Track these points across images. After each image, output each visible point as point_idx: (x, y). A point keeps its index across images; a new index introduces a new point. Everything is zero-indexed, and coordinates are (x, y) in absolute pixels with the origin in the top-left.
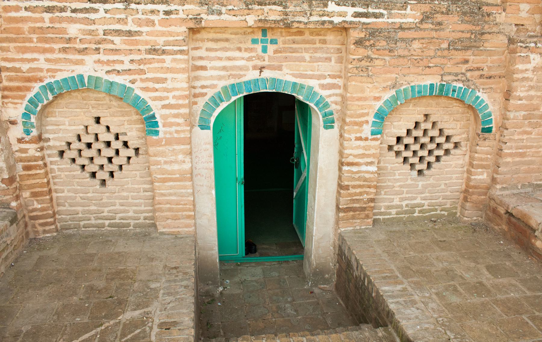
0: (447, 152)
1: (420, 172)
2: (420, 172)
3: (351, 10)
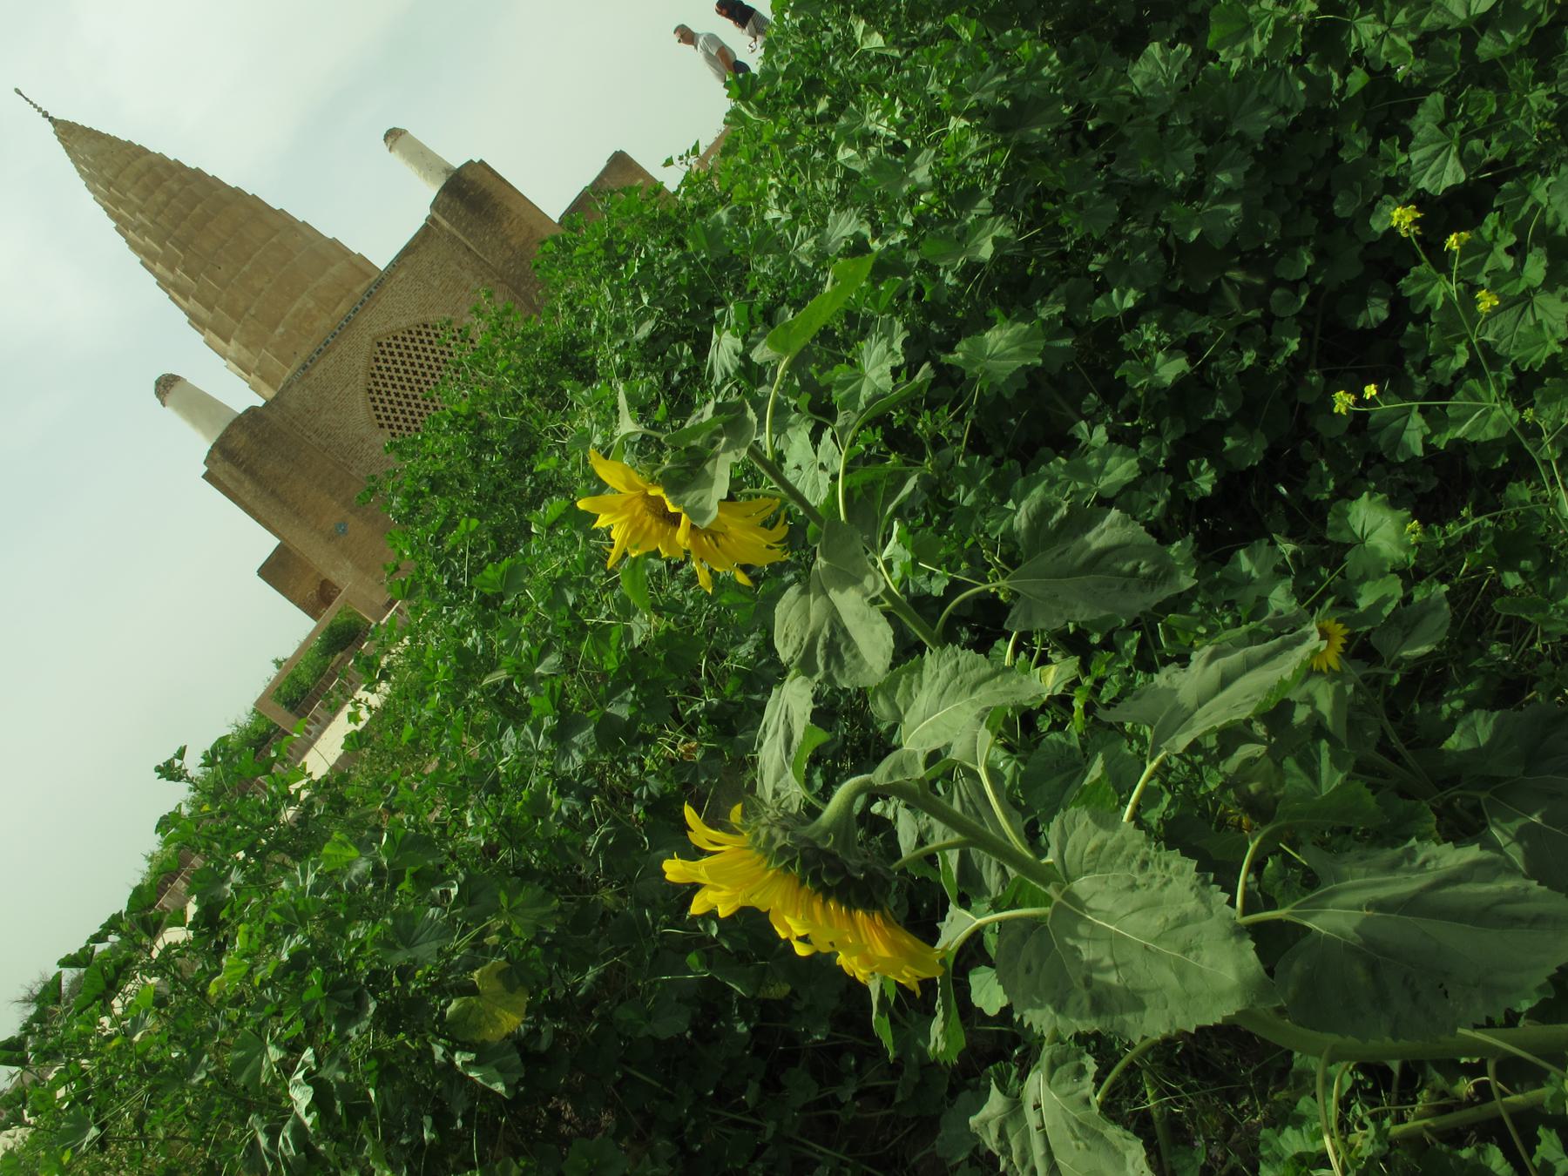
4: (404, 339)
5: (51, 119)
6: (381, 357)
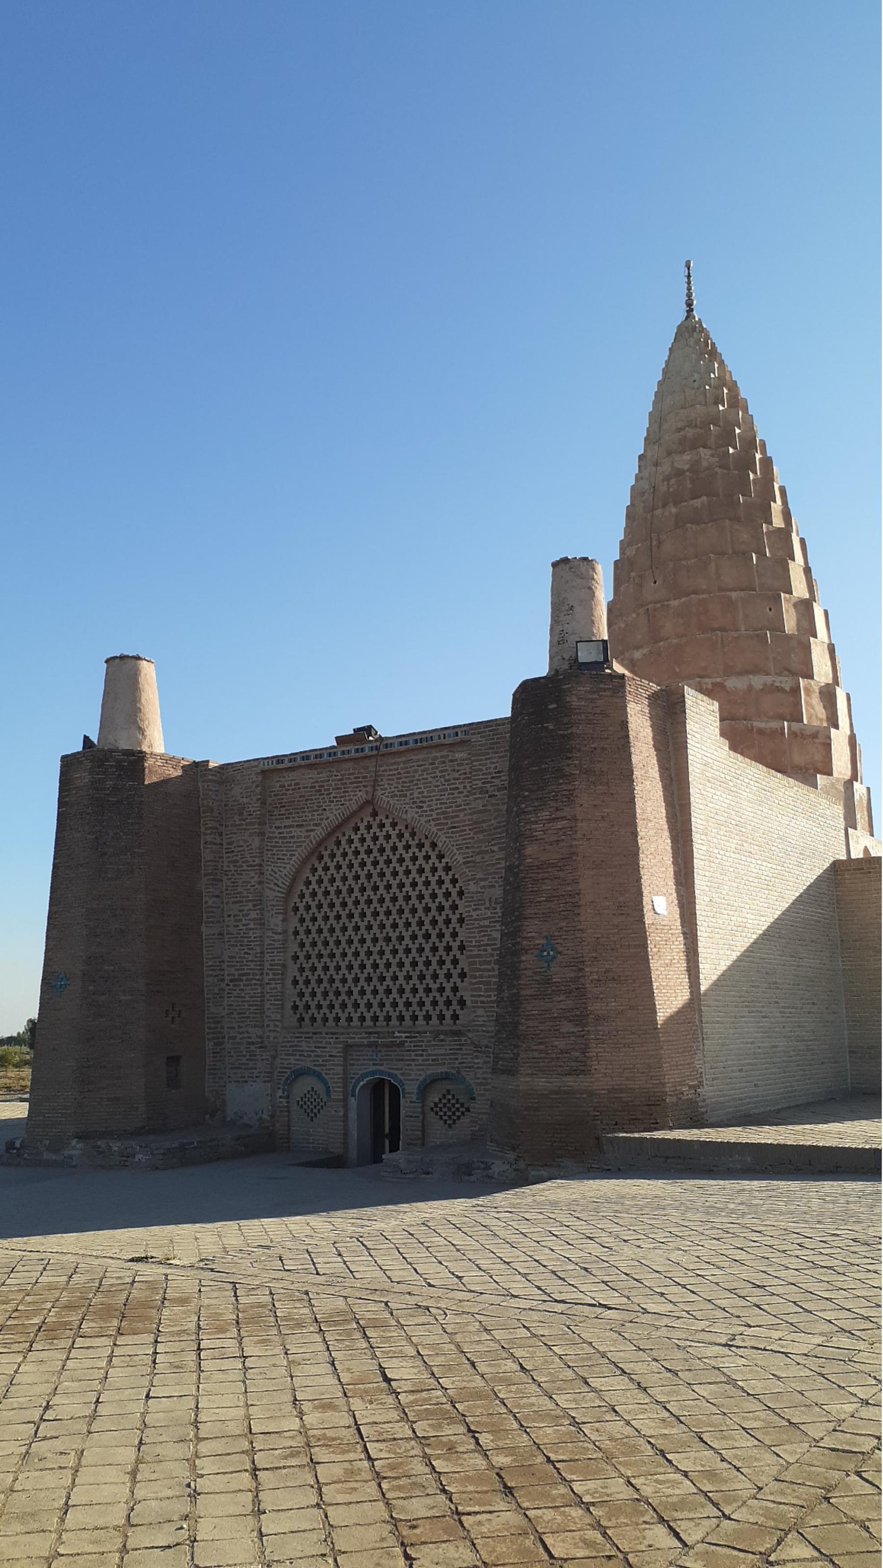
0: (463, 1113)
1: (450, 1125)
2: (450, 1125)
3: (404, 1035)
4: (400, 836)
5: (690, 310)
6: (363, 830)
